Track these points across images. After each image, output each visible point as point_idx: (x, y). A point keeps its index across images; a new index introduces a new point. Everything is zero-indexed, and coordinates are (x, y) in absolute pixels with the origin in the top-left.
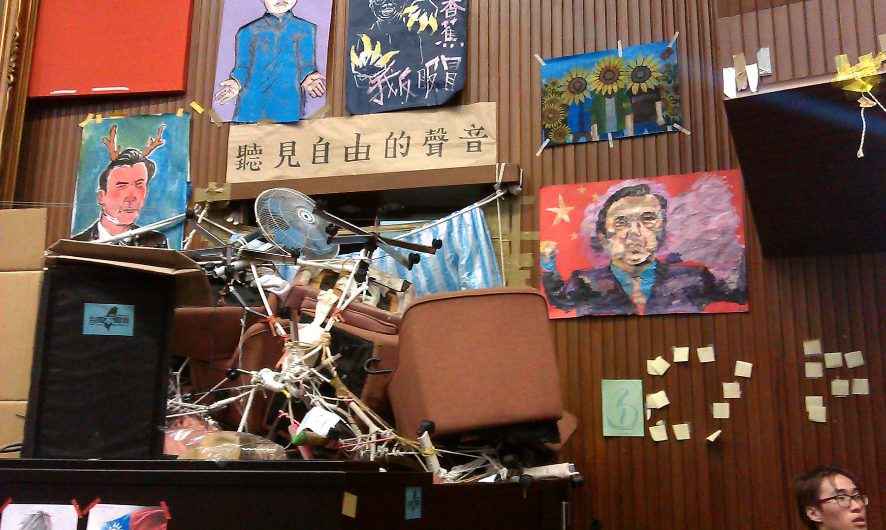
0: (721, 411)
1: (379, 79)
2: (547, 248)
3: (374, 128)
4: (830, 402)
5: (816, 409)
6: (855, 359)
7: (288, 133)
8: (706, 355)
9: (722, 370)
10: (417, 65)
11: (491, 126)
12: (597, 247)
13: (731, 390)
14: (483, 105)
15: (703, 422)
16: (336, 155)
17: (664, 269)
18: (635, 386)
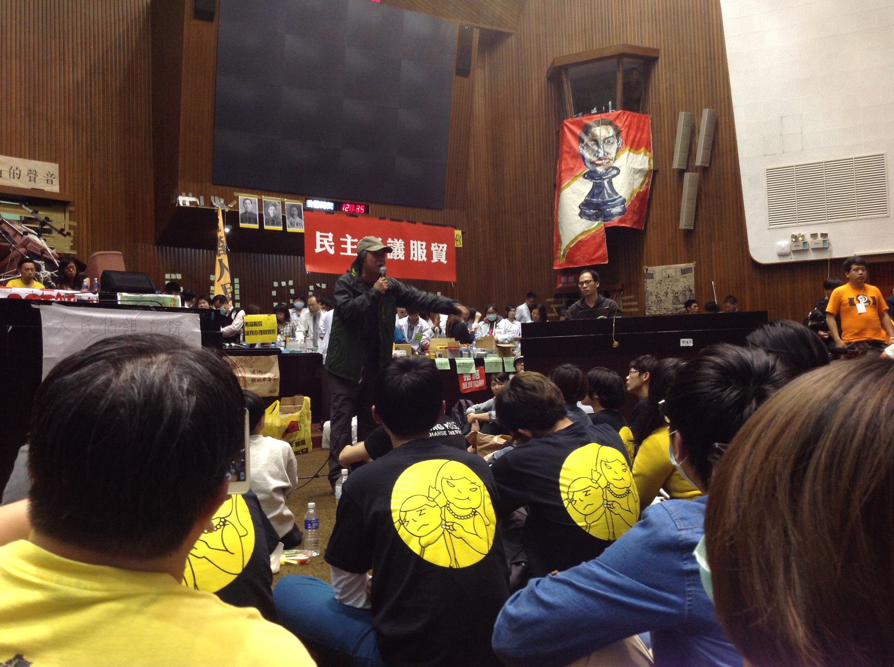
11: (57, 174)
14: (53, 164)
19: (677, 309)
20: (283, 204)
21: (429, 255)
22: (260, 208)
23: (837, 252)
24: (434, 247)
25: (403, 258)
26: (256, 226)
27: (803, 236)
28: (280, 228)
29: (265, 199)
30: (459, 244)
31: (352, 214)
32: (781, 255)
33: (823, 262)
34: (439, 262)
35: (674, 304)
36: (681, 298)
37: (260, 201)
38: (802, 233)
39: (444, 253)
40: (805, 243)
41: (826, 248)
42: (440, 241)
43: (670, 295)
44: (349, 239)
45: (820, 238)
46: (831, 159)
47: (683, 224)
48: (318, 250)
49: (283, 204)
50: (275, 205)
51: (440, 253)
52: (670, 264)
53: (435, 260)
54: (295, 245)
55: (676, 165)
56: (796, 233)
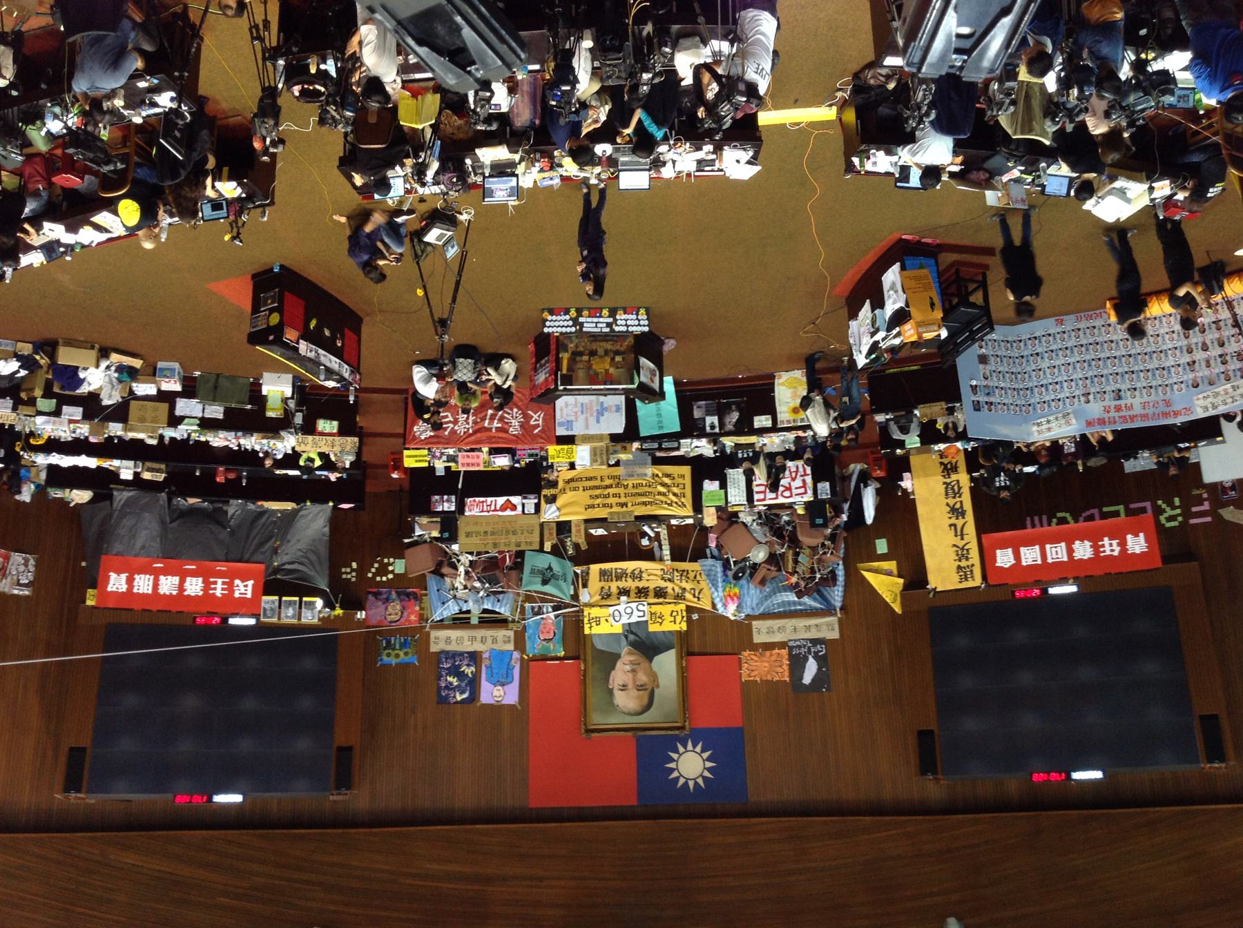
0: (376, 565)
1: (466, 662)
2: (417, 608)
3: (468, 647)
4: (350, 566)
5: (354, 565)
6: (344, 576)
7: (494, 646)
8: (378, 579)
9: (375, 575)
10: (453, 664)
11: (432, 645)
12: (404, 608)
13: (373, 570)
15: (381, 563)
16: (479, 639)
17: (387, 600)
18: (397, 571)
20: (279, 618)
21: (130, 581)
22: (300, 614)
24: (123, 588)
25: (162, 578)
26: (305, 599)
28: (284, 598)
29: (295, 621)
30: (90, 592)
31: (214, 614)
34: (119, 572)
37: (300, 619)
39: (112, 581)
42: (115, 594)
44: (218, 593)
48: (250, 583)
49: (279, 618)
50: (287, 617)
51: (117, 583)
53: (124, 576)
54: (272, 586)
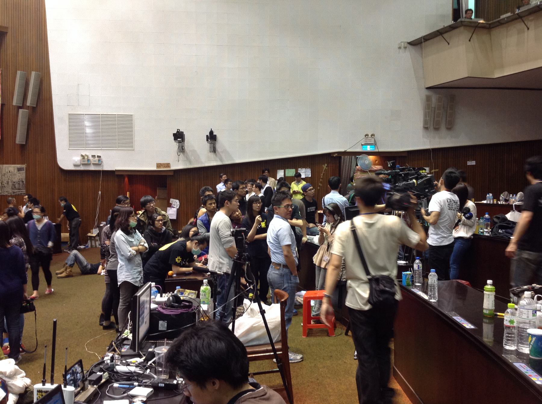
19: (14, 193)
23: (107, 167)
27: (87, 156)
32: (75, 166)
33: (99, 172)
35: (12, 189)
36: (17, 186)
38: (87, 154)
40: (88, 160)
41: (101, 164)
43: (10, 184)
45: (97, 159)
46: (105, 113)
47: (18, 141)
52: (10, 164)
55: (15, 103)
56: (84, 154)
